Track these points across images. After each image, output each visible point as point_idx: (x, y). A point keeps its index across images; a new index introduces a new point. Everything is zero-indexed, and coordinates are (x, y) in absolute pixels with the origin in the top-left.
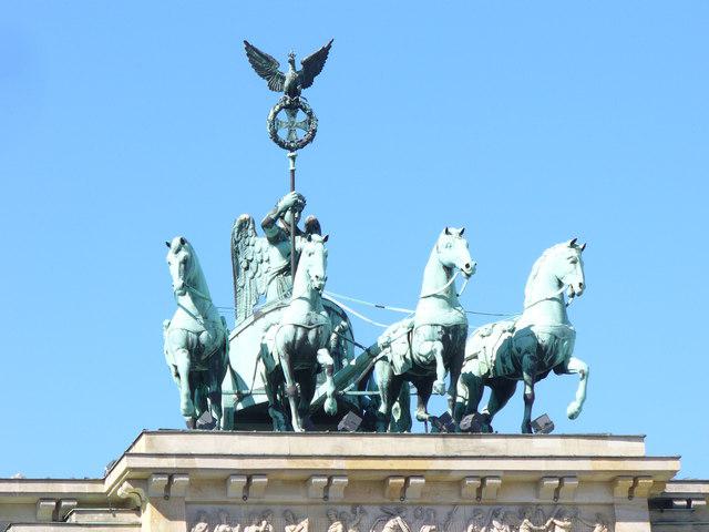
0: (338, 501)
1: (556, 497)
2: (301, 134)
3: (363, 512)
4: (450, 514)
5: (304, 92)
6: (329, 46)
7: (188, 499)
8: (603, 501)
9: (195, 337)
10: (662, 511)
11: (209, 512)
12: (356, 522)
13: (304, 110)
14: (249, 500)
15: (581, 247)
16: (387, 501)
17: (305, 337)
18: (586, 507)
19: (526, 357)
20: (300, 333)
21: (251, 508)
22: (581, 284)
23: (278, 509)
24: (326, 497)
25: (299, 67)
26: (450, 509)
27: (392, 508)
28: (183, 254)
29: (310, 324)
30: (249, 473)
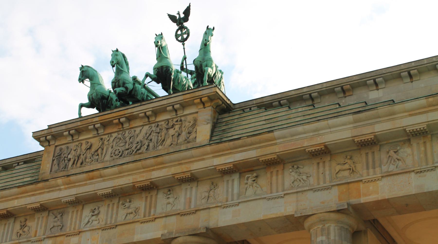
1: (177, 115)
2: (185, 36)
3: (111, 136)
4: (141, 130)
6: (190, 6)
7: (56, 144)
9: (91, 97)
15: (212, 28)
24: (98, 134)
25: (182, 16)
26: (141, 128)
29: (116, 80)
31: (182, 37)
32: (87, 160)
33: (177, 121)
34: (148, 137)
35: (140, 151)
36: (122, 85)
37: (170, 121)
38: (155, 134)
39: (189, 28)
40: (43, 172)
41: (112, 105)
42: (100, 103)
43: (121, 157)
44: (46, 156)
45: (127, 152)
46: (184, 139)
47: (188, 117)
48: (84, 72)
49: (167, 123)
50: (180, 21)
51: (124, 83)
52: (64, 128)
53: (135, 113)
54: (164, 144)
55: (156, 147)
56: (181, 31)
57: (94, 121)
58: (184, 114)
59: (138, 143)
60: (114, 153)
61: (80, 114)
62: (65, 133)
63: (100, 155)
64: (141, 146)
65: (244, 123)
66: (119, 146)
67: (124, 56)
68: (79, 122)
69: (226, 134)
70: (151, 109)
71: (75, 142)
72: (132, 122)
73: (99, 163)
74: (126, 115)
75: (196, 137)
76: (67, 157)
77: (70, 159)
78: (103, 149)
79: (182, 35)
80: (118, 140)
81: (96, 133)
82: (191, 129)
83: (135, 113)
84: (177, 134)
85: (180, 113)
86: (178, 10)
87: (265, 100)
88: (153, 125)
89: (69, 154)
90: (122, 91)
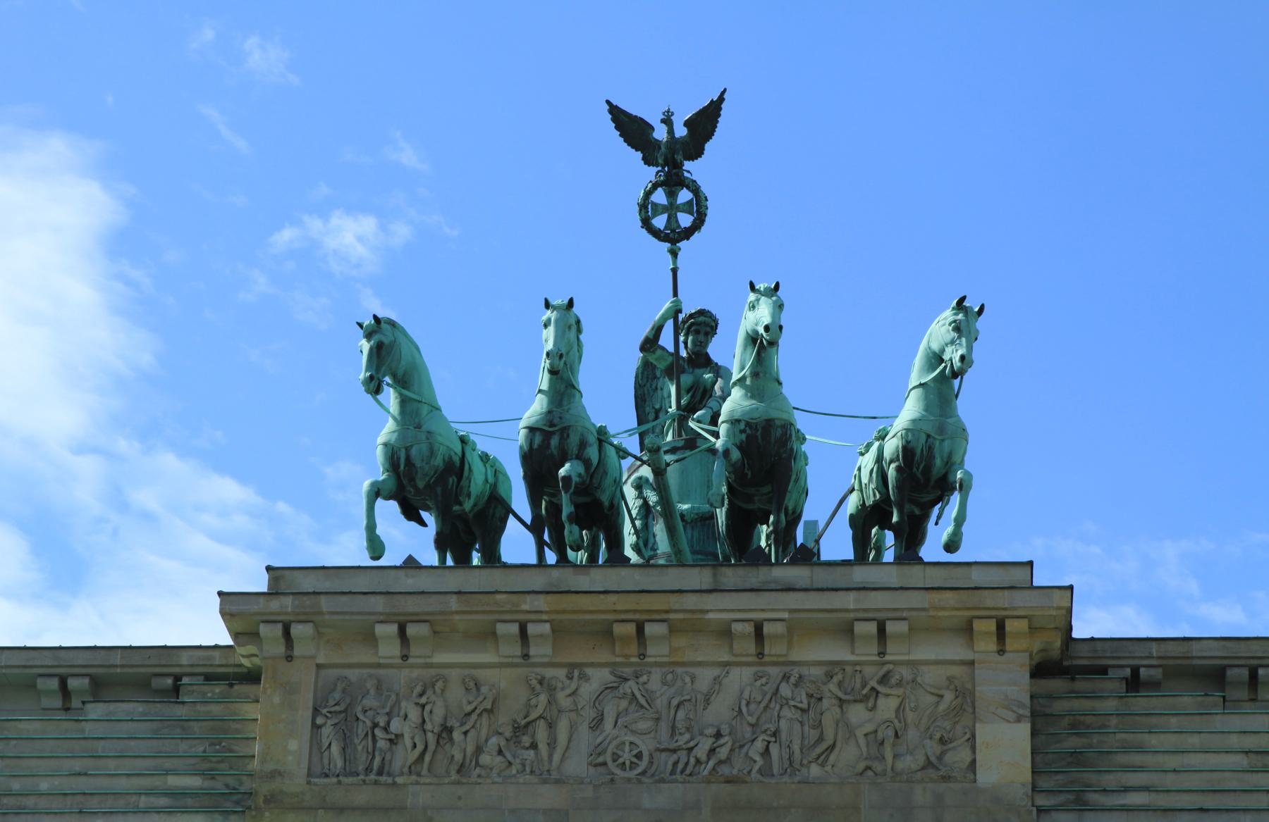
0: (545, 660)
1: (882, 653)
2: (685, 220)
3: (584, 677)
4: (717, 680)
5: (688, 165)
6: (721, 99)
7: (320, 660)
8: (957, 658)
10: (1073, 679)
11: (353, 679)
12: (569, 691)
13: (688, 188)
14: (411, 661)
16: (619, 660)
17: (545, 444)
18: (932, 667)
19: (893, 466)
20: (538, 439)
21: (416, 673)
22: (963, 358)
23: (454, 674)
24: (526, 656)
25: (681, 131)
26: (716, 671)
27: (627, 671)
28: (376, 338)
29: (552, 425)
30: (401, 618)
31: (672, 219)
32: (485, 759)
33: (884, 680)
34: (758, 719)
35: (725, 770)
36: (575, 451)
37: (849, 669)
38: (786, 712)
39: (705, 189)
40: (270, 767)
41: (469, 495)
42: (439, 490)
43: (645, 779)
44: (277, 700)
45: (666, 761)
46: (921, 760)
47: (924, 668)
48: (384, 353)
49: (840, 676)
50: (673, 152)
51: (583, 444)
52: (380, 609)
53: (711, 616)
54: (832, 758)
55: (797, 765)
56: (672, 195)
57: (526, 607)
58: (912, 657)
59: (718, 735)
60: (615, 757)
61: (371, 527)
62: (380, 629)
63: (543, 747)
64: (732, 750)
65: (1154, 741)
66: (634, 732)
67: (578, 322)
68: (454, 599)
69: (1093, 778)
70: (786, 615)
71: (412, 666)
72: (681, 641)
73: (545, 782)
74: (672, 616)
75: (974, 761)
76: (386, 729)
77: (399, 736)
78: (551, 726)
79: (674, 213)
80: (624, 704)
81: (518, 651)
82: (947, 725)
83: (711, 616)
84: (891, 733)
85: (895, 652)
86: (666, 102)
87: (1196, 649)
88: (774, 671)
89: (389, 715)
90: (580, 475)
